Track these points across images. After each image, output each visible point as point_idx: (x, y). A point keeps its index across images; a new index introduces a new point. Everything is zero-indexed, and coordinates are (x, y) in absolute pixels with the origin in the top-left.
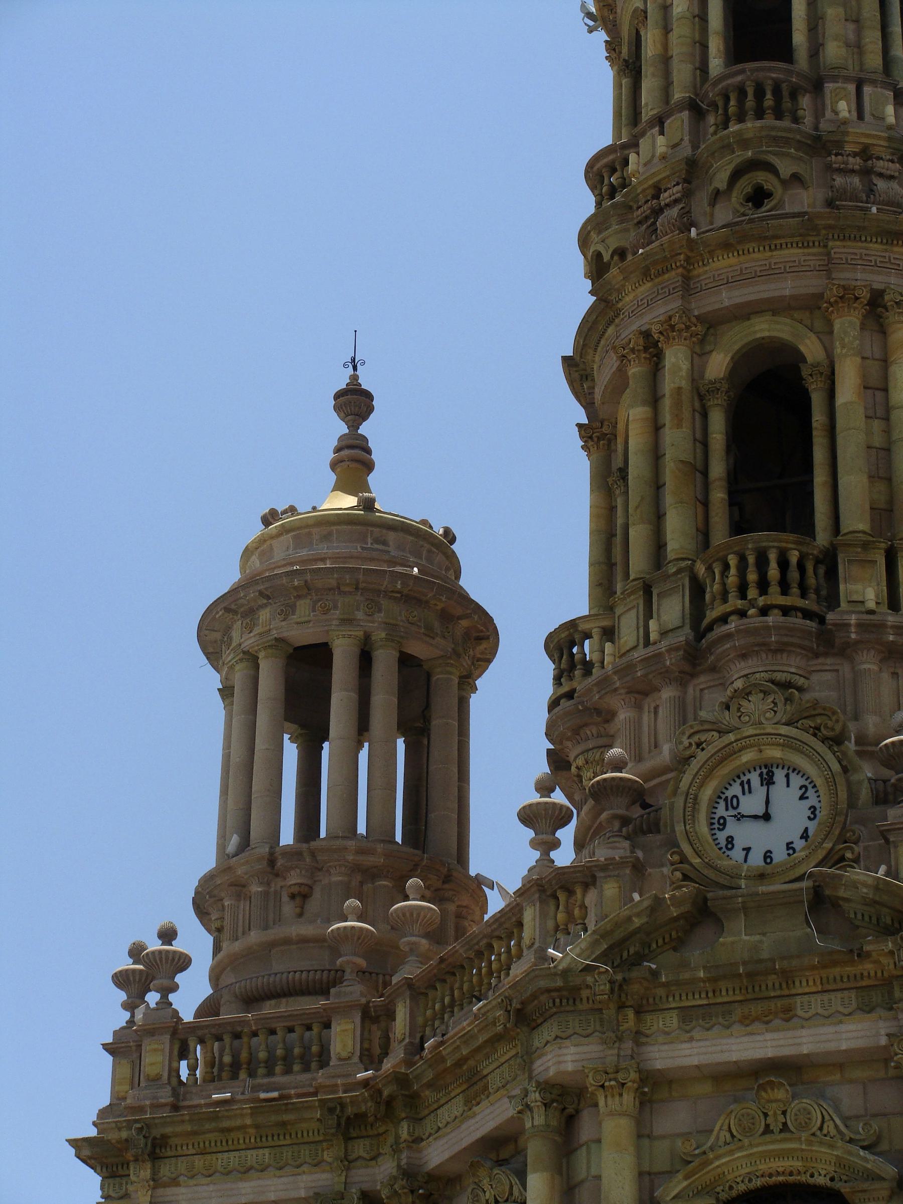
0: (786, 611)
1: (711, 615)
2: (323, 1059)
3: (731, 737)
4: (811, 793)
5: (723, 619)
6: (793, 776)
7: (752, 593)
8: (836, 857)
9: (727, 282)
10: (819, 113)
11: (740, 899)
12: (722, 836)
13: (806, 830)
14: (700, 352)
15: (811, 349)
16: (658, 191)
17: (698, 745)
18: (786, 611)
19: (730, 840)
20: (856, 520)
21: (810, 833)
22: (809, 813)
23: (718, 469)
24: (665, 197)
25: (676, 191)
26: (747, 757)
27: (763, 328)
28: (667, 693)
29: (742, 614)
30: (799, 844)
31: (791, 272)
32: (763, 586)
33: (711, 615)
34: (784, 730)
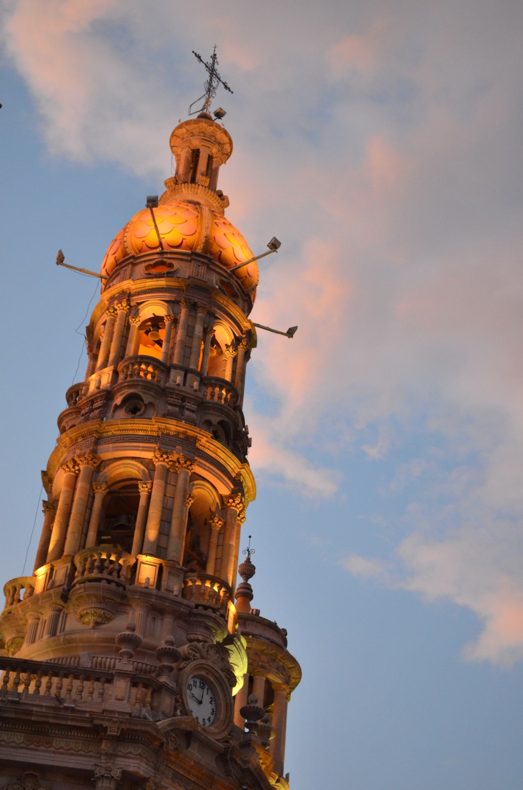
3: (204, 661)
4: (213, 702)
5: (206, 608)
6: (209, 691)
8: (225, 740)
11: (202, 737)
13: (210, 718)
17: (194, 656)
21: (212, 720)
22: (211, 711)
24: (188, 405)
25: (194, 407)
26: (203, 673)
28: (168, 620)
30: (207, 721)
34: (220, 672)
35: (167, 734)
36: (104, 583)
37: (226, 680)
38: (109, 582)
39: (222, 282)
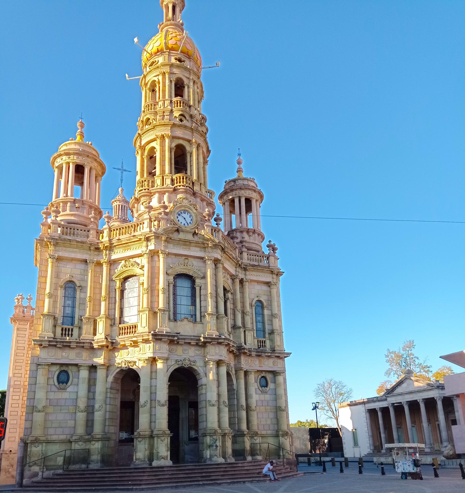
0: (190, 188)
1: (176, 185)
2: (88, 237)
3: (180, 205)
5: (180, 186)
7: (185, 183)
9: (179, 133)
10: (190, 110)
12: (177, 219)
14: (171, 142)
15: (188, 148)
16: (164, 112)
18: (190, 188)
19: (179, 220)
20: (195, 177)
23: (173, 162)
26: (183, 208)
27: (181, 142)
29: (183, 186)
30: (189, 224)
31: (187, 134)
32: (186, 182)
33: (176, 185)
35: (162, 234)
36: (144, 191)
37: (192, 208)
38: (145, 190)
39: (176, 59)
